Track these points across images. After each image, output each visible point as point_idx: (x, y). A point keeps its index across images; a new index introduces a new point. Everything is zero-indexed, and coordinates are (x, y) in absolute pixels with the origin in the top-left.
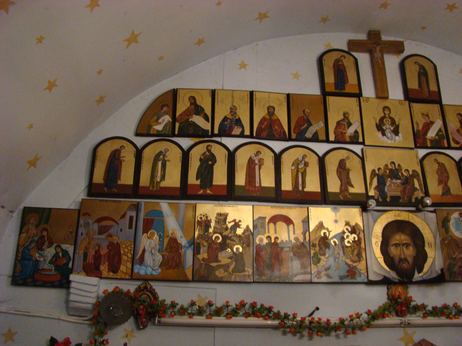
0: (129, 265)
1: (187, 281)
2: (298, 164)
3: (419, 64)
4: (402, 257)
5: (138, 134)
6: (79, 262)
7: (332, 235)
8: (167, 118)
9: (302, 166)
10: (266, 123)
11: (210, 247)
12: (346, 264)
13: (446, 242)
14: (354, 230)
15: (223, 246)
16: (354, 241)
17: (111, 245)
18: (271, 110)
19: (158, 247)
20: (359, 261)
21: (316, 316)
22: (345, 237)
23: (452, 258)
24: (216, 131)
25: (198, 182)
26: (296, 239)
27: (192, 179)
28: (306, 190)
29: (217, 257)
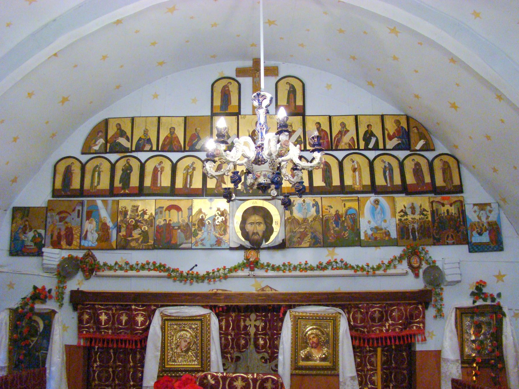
0: (78, 240)
1: (114, 249)
2: (188, 169)
3: (290, 84)
4: (255, 232)
5: (83, 153)
6: (48, 240)
7: (207, 217)
8: (102, 141)
9: (191, 170)
10: (168, 140)
11: (127, 228)
12: (216, 236)
13: (290, 221)
14: (222, 214)
15: (136, 227)
16: (222, 221)
17: (67, 228)
18: (172, 130)
19: (95, 229)
21: (195, 270)
22: (216, 219)
23: (293, 232)
24: (134, 149)
25: (121, 185)
26: (183, 221)
27: (117, 183)
28: (191, 187)
29: (131, 233)
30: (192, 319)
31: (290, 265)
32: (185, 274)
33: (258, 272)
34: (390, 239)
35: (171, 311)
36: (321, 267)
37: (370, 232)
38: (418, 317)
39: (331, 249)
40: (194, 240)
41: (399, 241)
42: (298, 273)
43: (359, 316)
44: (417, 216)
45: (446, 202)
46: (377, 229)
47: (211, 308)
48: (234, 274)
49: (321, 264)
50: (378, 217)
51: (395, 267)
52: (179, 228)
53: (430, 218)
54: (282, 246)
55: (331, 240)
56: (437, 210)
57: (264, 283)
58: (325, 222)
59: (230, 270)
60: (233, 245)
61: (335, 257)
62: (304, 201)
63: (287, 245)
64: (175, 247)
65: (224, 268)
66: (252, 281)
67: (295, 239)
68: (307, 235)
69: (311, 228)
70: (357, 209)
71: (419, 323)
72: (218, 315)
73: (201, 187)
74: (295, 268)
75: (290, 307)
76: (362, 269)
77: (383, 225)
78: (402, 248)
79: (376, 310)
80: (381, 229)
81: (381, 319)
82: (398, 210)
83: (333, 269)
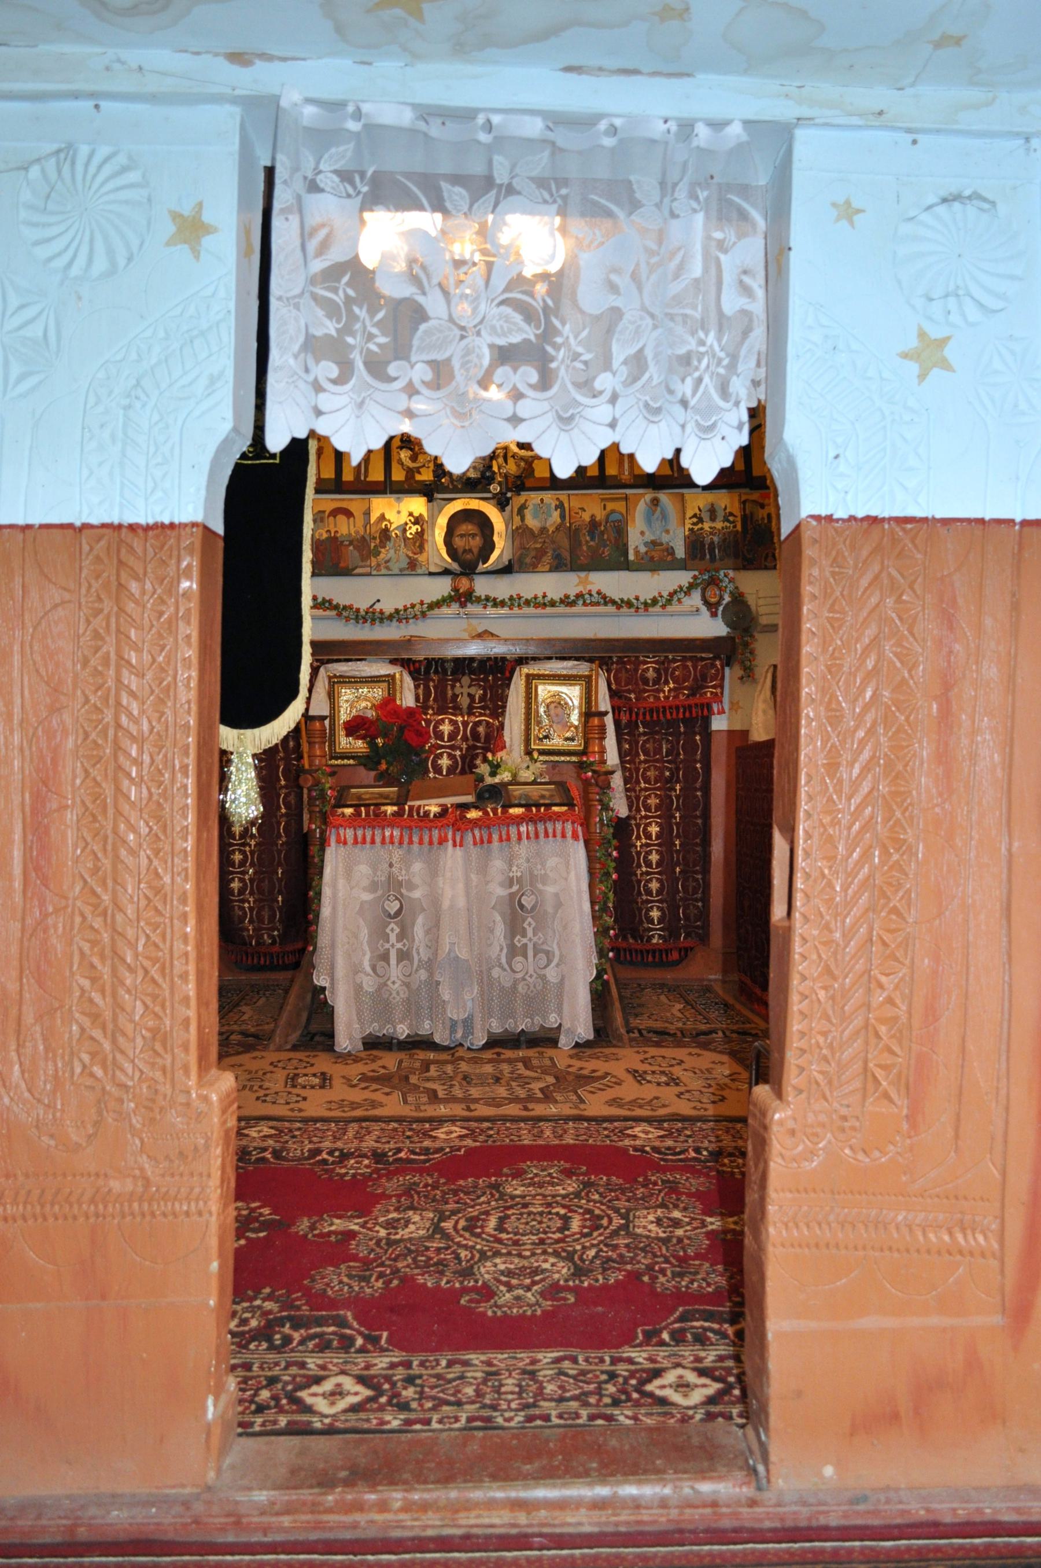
7: (393, 526)
20: (421, 552)
21: (378, 607)
26: (357, 532)
30: (373, 680)
31: (520, 598)
32: (363, 613)
33: (471, 608)
36: (567, 601)
37: (643, 549)
39: (583, 574)
40: (374, 562)
42: (531, 610)
43: (623, 675)
44: (719, 525)
46: (654, 543)
47: (405, 663)
48: (436, 611)
49: (567, 597)
52: (351, 543)
53: (739, 528)
54: (507, 570)
55: (583, 560)
56: (752, 514)
58: (573, 534)
60: (433, 569)
61: (589, 587)
62: (542, 500)
63: (516, 567)
64: (346, 572)
65: (422, 603)
69: (553, 542)
70: (624, 511)
71: (714, 687)
72: (415, 675)
73: (382, 478)
74: (527, 603)
75: (522, 661)
76: (629, 604)
77: (665, 538)
78: (691, 574)
80: (661, 544)
81: (657, 681)
82: (689, 514)
83: (585, 604)
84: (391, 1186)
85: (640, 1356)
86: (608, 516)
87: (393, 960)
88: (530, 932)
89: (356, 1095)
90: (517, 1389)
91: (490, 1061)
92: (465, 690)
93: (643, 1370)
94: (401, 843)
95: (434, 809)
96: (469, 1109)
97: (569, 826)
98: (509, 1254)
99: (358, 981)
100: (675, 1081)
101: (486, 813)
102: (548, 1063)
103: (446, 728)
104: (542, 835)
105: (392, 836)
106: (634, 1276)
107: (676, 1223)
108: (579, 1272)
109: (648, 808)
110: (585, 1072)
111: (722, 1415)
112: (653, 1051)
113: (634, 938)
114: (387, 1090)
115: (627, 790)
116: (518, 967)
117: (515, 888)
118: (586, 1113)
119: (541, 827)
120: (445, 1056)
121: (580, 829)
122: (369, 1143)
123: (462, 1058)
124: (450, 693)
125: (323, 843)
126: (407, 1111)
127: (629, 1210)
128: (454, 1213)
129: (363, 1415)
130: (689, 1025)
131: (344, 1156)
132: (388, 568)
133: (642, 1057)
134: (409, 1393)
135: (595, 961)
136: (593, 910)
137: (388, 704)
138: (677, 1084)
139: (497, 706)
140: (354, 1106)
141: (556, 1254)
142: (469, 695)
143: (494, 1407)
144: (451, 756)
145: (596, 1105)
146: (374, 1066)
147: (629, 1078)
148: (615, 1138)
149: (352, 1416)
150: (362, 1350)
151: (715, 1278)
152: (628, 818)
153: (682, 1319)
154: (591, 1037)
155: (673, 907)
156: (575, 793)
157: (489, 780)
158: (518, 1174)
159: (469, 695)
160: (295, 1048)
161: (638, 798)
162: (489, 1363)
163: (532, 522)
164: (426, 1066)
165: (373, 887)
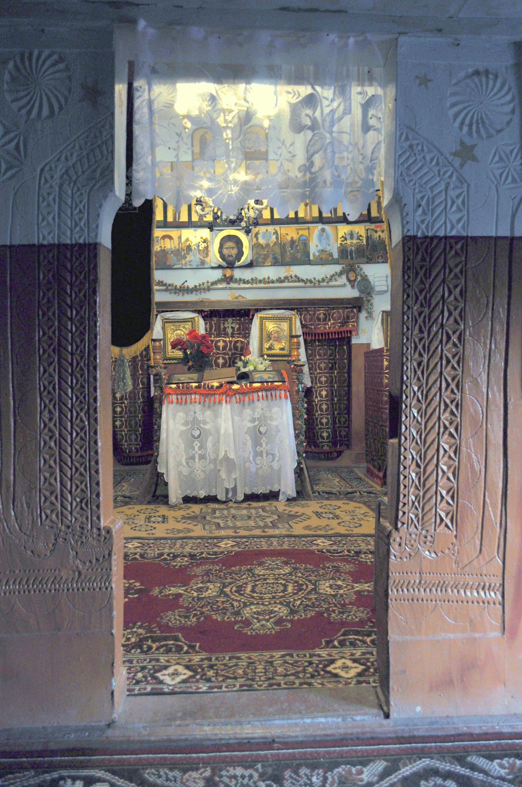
14: (205, 241)
20: (207, 257)
26: (175, 247)
30: (185, 321)
31: (256, 279)
32: (178, 287)
34: (333, 259)
35: (169, 315)
36: (280, 280)
37: (317, 254)
38: (352, 318)
39: (287, 267)
41: (340, 260)
42: (262, 285)
43: (308, 317)
44: (355, 241)
45: (378, 229)
46: (322, 251)
47: (200, 312)
48: (215, 286)
50: (324, 242)
51: (336, 280)
52: (172, 252)
53: (365, 243)
54: (250, 265)
55: (288, 260)
57: (237, 293)
58: (283, 247)
59: (213, 284)
60: (213, 265)
61: (291, 273)
63: (254, 264)
64: (170, 268)
66: (228, 292)
67: (260, 260)
68: (269, 256)
69: (273, 251)
70: (307, 235)
71: (353, 322)
73: (187, 220)
74: (260, 282)
75: (257, 310)
76: (311, 282)
77: (328, 248)
78: (342, 266)
79: (321, 313)
80: (326, 251)
81: (325, 319)
82: (340, 236)
83: (289, 282)
84: (199, 571)
85: (324, 653)
86: (300, 237)
87: (197, 460)
88: (264, 445)
89: (180, 526)
90: (264, 671)
91: (246, 508)
92: (230, 324)
93: (326, 660)
94: (200, 403)
95: (216, 384)
96: (236, 532)
97: (283, 392)
98: (258, 603)
99: (180, 470)
100: (337, 517)
101: (242, 386)
102: (274, 509)
103: (221, 344)
104: (269, 396)
105: (195, 398)
106: (320, 614)
107: (340, 587)
108: (293, 612)
109: (321, 383)
110: (292, 513)
111: (365, 682)
112: (325, 502)
113: (315, 447)
114: (196, 523)
115: (310, 374)
116: (258, 462)
117: (257, 423)
118: (293, 533)
119: (269, 394)
120: (223, 506)
121: (288, 393)
122: (187, 550)
123: (231, 507)
124: (222, 327)
125: (161, 404)
126: (205, 533)
127: (316, 581)
128: (230, 584)
129: (188, 685)
130: (343, 489)
131: (175, 557)
132: (191, 265)
133: (320, 505)
134: (211, 673)
135: (297, 458)
136: (295, 433)
137: (192, 333)
138: (338, 518)
139: (246, 333)
140: (179, 531)
141: (281, 603)
142: (232, 327)
143: (253, 680)
144: (224, 358)
145: (298, 529)
146: (189, 511)
147: (314, 516)
148: (308, 546)
149: (182, 685)
150: (187, 652)
151: (359, 614)
152: (311, 387)
153: (344, 634)
154: (295, 495)
155: (334, 431)
156: (285, 376)
157: (243, 370)
158: (261, 564)
159: (232, 327)
160: (149, 503)
161: (316, 378)
162: (250, 658)
163: (261, 241)
164: (214, 511)
165: (186, 423)
